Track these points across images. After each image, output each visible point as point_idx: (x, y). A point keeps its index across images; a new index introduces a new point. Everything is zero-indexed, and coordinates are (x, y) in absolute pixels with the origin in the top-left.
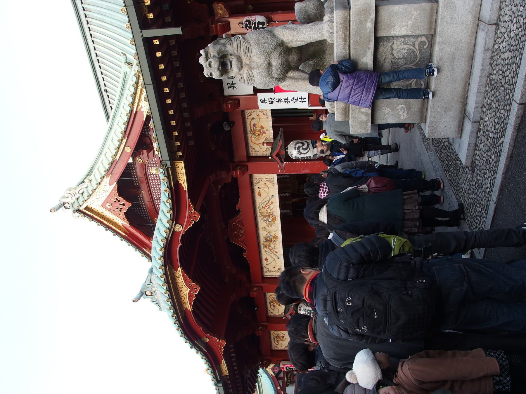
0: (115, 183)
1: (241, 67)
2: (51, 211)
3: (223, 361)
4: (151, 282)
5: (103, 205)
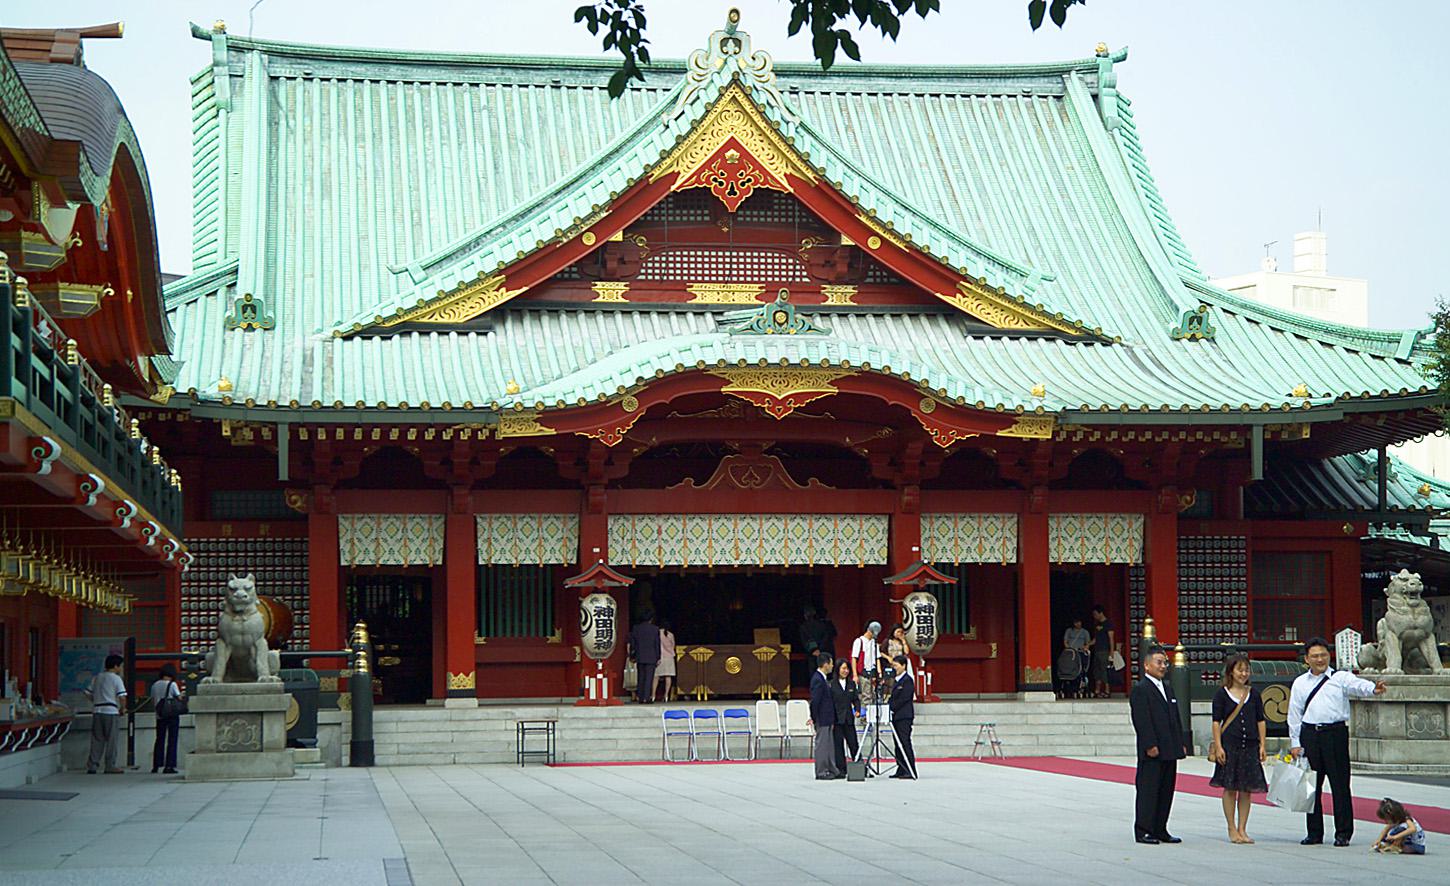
0: (792, 190)
1: (1411, 606)
2: (736, 11)
3: (552, 432)
4: (810, 329)
5: (732, 143)
